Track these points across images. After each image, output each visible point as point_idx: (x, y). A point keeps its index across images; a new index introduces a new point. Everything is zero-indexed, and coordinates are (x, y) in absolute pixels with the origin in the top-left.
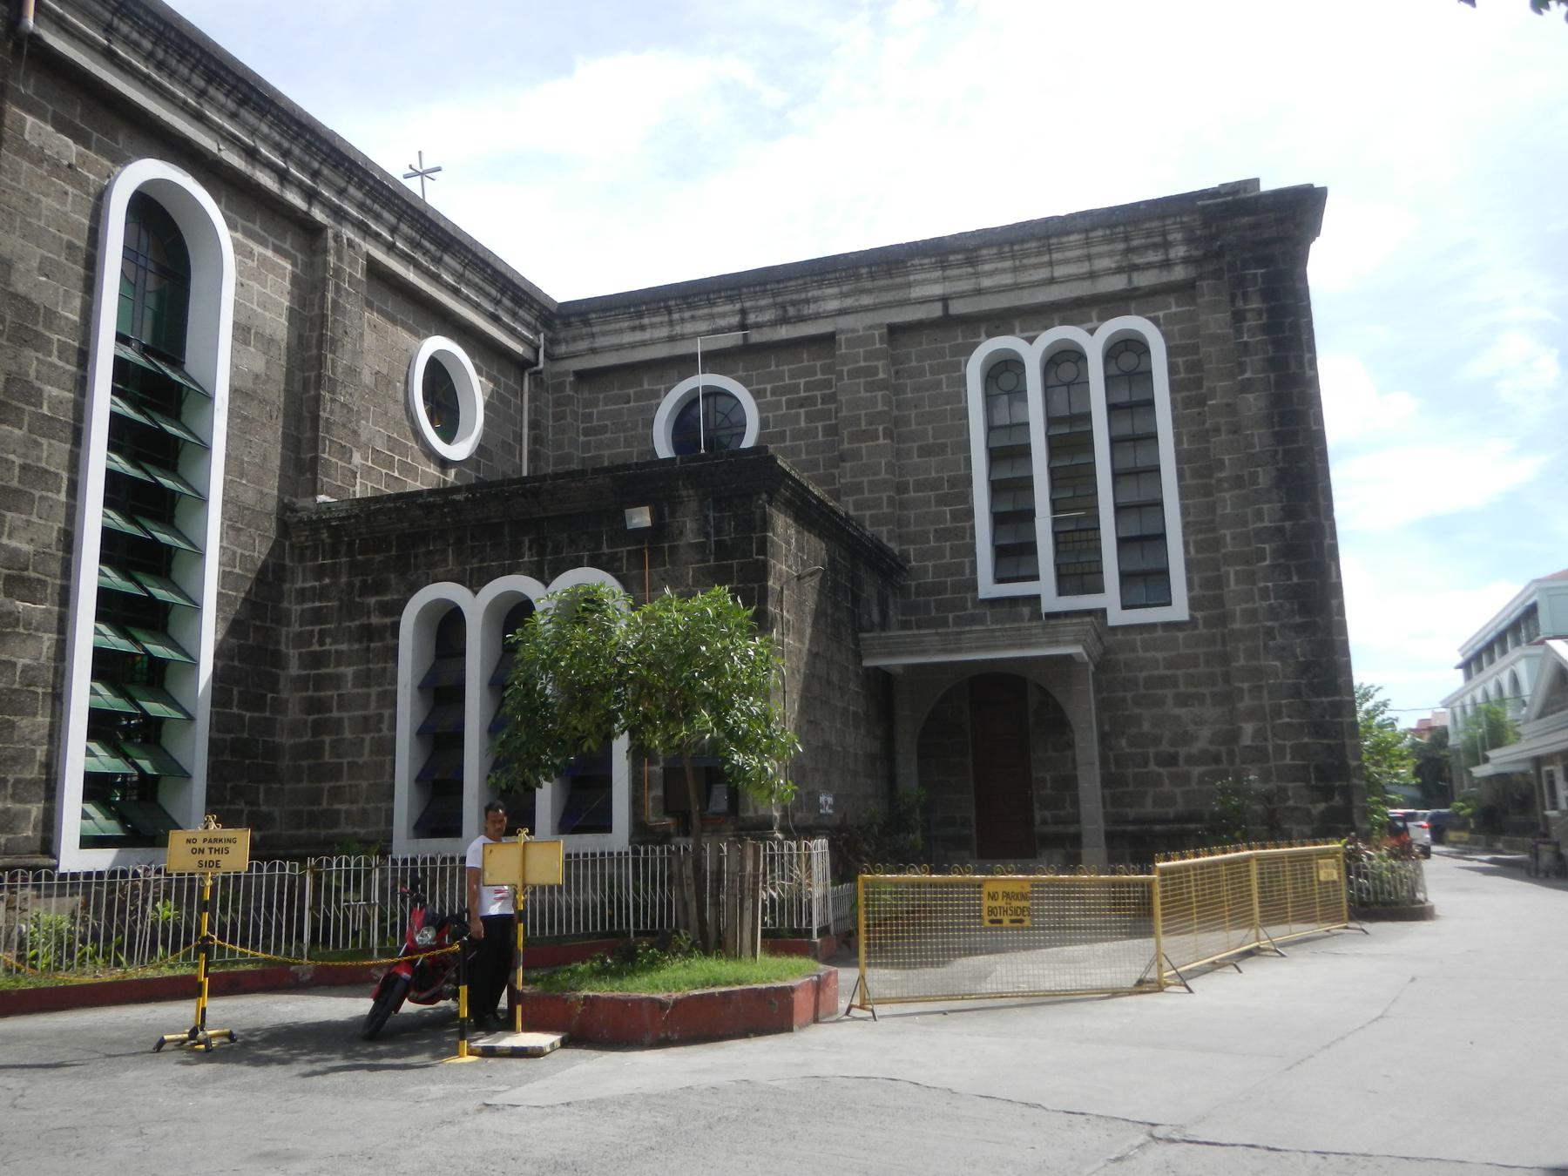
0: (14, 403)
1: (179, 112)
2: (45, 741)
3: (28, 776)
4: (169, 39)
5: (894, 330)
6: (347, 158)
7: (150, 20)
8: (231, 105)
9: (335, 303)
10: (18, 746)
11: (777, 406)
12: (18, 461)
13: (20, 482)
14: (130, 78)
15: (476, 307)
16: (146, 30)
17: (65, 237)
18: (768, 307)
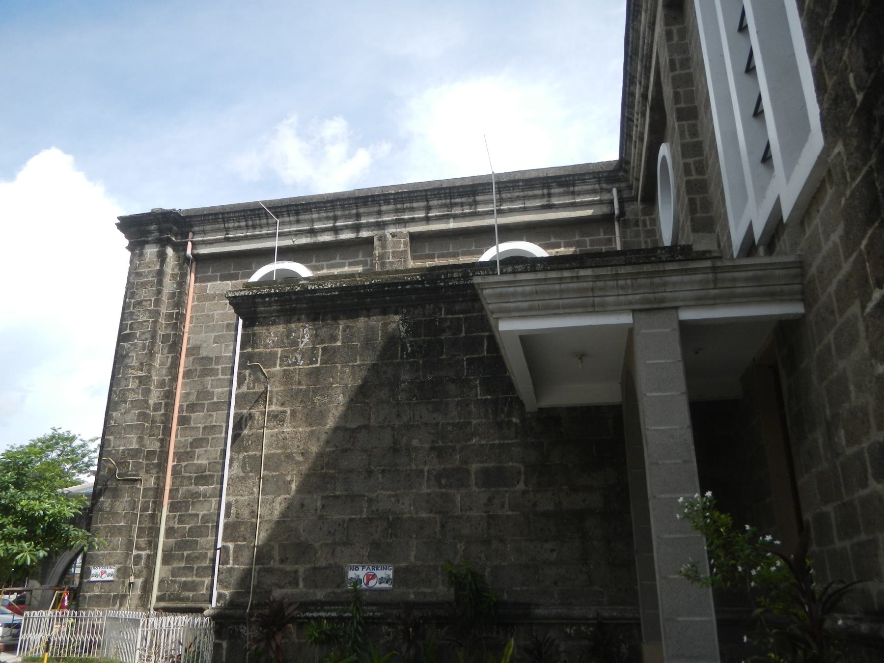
0: (200, 402)
1: (268, 239)
2: (213, 548)
3: (204, 565)
4: (248, 216)
6: (367, 197)
7: (236, 214)
8: (292, 218)
10: (199, 551)
12: (201, 426)
13: (202, 435)
14: (241, 242)
15: (525, 210)
16: (239, 219)
17: (225, 323)
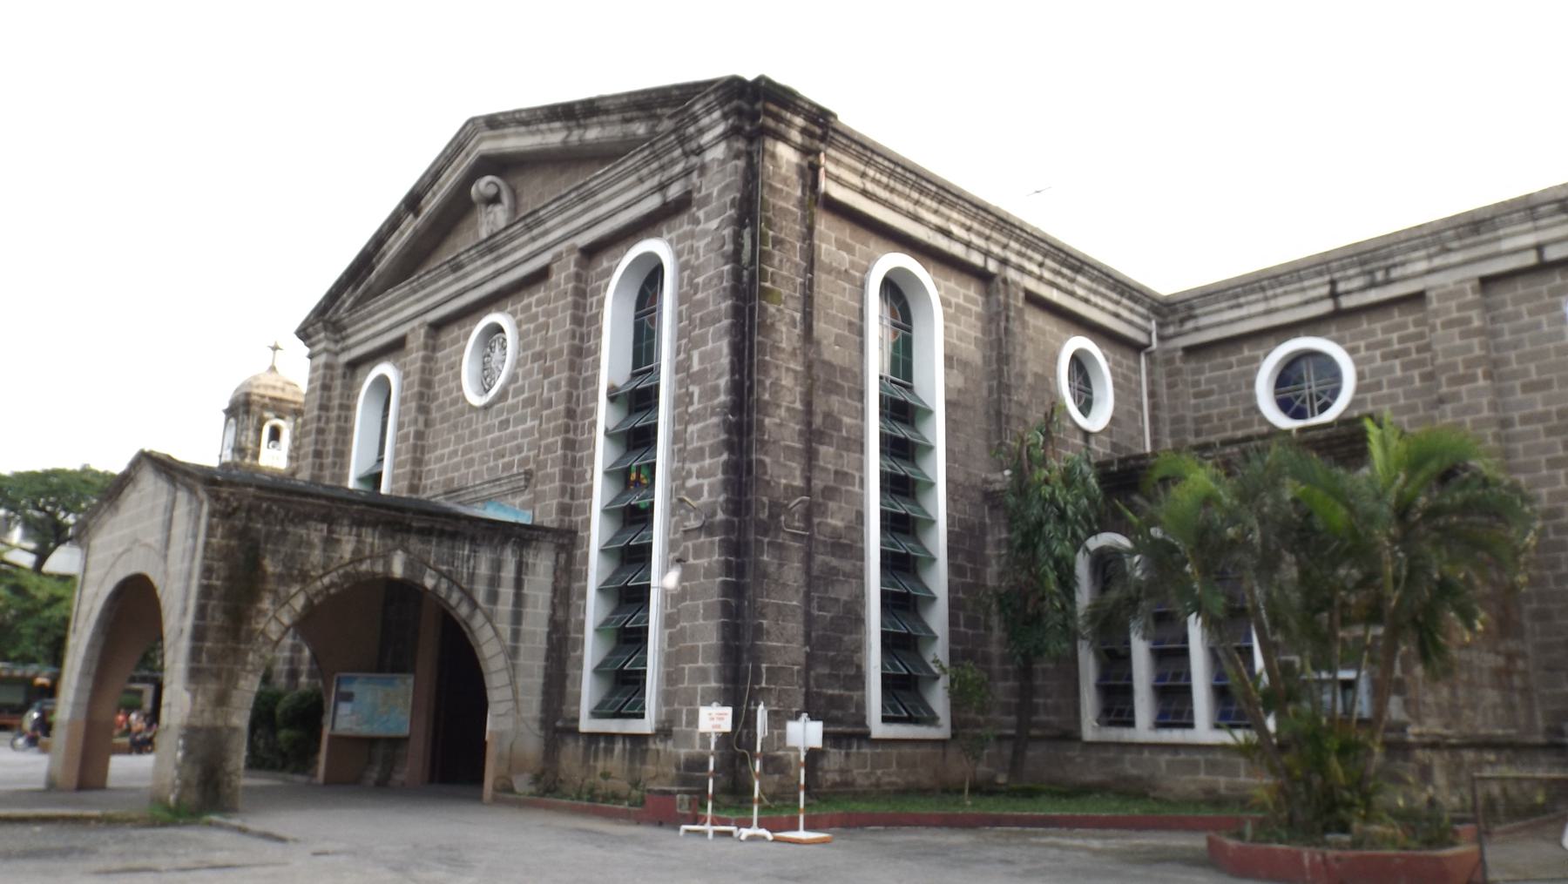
5: (1486, 282)
9: (1006, 329)
11: (1371, 360)
15: (1103, 309)
17: (846, 317)
18: (1357, 275)
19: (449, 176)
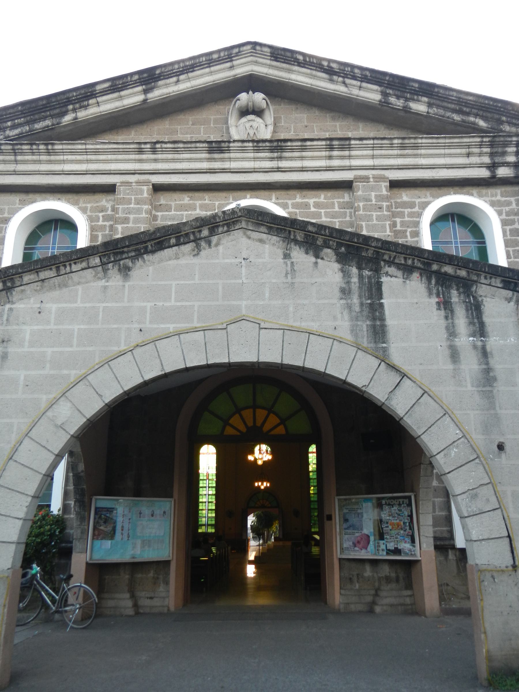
19: (202, 75)
